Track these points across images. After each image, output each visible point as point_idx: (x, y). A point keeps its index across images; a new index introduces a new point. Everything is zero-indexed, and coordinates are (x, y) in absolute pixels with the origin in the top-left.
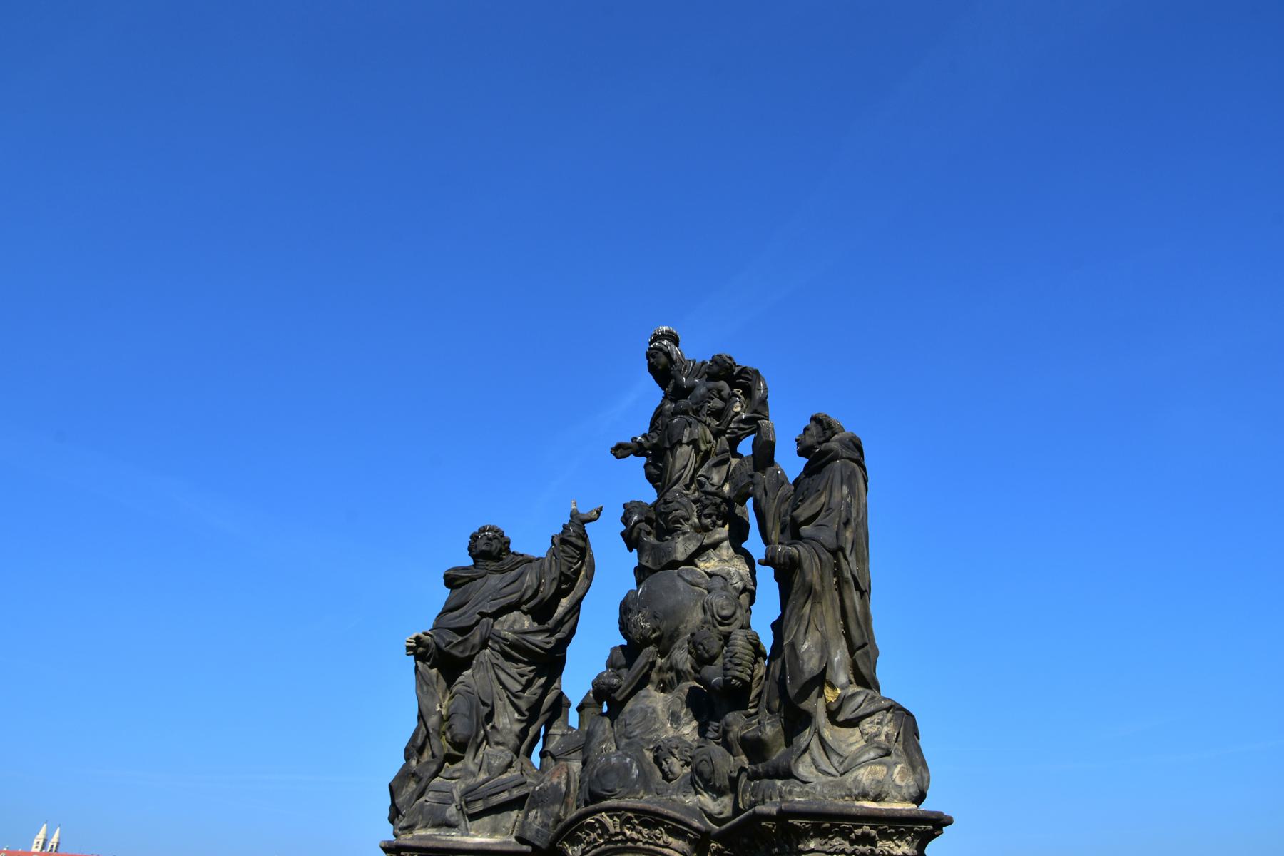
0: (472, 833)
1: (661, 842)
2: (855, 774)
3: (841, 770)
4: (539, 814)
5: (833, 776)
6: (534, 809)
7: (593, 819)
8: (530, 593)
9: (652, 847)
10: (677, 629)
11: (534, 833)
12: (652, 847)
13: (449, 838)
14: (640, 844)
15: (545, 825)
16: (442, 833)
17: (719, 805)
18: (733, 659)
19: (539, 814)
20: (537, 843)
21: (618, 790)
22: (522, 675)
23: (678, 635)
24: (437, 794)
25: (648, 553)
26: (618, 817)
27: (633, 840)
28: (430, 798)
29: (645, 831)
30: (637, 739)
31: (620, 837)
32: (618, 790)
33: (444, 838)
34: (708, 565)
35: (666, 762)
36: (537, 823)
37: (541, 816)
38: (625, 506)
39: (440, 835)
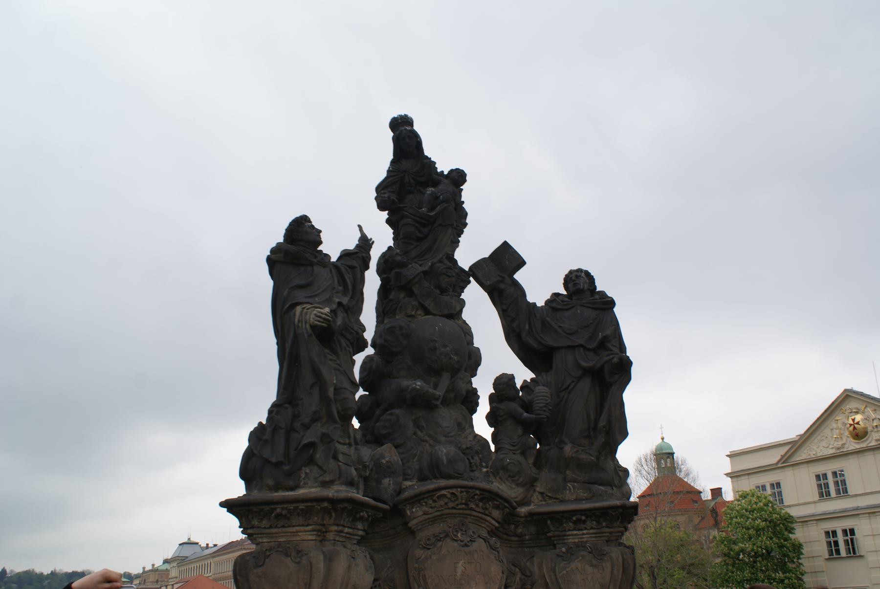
1: (487, 512)
6: (386, 477)
7: (447, 492)
9: (480, 515)
12: (480, 515)
14: (475, 513)
19: (391, 482)
26: (467, 492)
27: (472, 509)
29: (481, 504)
37: (393, 483)
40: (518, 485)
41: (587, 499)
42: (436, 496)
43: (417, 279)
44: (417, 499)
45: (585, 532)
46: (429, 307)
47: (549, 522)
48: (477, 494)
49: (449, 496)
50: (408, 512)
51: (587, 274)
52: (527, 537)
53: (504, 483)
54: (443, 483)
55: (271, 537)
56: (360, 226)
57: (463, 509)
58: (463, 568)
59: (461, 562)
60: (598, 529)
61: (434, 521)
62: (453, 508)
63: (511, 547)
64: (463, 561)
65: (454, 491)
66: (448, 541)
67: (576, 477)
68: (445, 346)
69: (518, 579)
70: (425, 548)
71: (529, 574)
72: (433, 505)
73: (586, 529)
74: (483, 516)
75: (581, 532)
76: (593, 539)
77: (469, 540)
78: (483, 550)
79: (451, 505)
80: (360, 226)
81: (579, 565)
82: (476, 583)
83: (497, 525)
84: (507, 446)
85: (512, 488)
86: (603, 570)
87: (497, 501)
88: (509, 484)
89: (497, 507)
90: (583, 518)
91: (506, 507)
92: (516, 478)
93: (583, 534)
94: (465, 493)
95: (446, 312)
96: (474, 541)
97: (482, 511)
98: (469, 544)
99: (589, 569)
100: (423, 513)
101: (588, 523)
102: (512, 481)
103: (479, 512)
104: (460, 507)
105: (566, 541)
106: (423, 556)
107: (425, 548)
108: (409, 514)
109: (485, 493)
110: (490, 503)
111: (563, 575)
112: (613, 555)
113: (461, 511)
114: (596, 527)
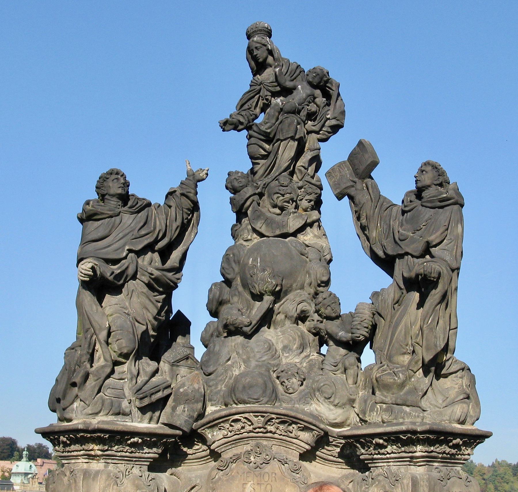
1: (292, 435)
5: (438, 408)
6: (180, 404)
8: (161, 235)
9: (284, 438)
10: (291, 286)
12: (284, 438)
14: (276, 436)
17: (334, 414)
18: (362, 323)
19: (186, 409)
20: (185, 429)
21: (261, 399)
23: (291, 291)
24: (113, 390)
25: (263, 221)
27: (271, 432)
28: (109, 393)
29: (281, 427)
31: (262, 430)
32: (261, 399)
33: (122, 423)
34: (305, 238)
36: (185, 415)
39: (118, 421)
42: (231, 420)
43: (248, 203)
44: (214, 424)
45: (388, 456)
48: (273, 418)
49: (244, 420)
50: (210, 436)
51: (435, 167)
53: (322, 404)
54: (241, 407)
58: (252, 489)
59: (250, 483)
62: (251, 432)
64: (252, 482)
65: (246, 415)
67: (384, 398)
72: (231, 428)
73: (388, 453)
77: (261, 462)
78: (276, 472)
79: (248, 428)
88: (327, 405)
89: (305, 429)
90: (381, 441)
92: (331, 400)
93: (388, 458)
94: (260, 417)
95: (278, 232)
97: (286, 434)
98: (261, 466)
104: (257, 430)
109: (282, 417)
113: (261, 434)
114: (396, 452)
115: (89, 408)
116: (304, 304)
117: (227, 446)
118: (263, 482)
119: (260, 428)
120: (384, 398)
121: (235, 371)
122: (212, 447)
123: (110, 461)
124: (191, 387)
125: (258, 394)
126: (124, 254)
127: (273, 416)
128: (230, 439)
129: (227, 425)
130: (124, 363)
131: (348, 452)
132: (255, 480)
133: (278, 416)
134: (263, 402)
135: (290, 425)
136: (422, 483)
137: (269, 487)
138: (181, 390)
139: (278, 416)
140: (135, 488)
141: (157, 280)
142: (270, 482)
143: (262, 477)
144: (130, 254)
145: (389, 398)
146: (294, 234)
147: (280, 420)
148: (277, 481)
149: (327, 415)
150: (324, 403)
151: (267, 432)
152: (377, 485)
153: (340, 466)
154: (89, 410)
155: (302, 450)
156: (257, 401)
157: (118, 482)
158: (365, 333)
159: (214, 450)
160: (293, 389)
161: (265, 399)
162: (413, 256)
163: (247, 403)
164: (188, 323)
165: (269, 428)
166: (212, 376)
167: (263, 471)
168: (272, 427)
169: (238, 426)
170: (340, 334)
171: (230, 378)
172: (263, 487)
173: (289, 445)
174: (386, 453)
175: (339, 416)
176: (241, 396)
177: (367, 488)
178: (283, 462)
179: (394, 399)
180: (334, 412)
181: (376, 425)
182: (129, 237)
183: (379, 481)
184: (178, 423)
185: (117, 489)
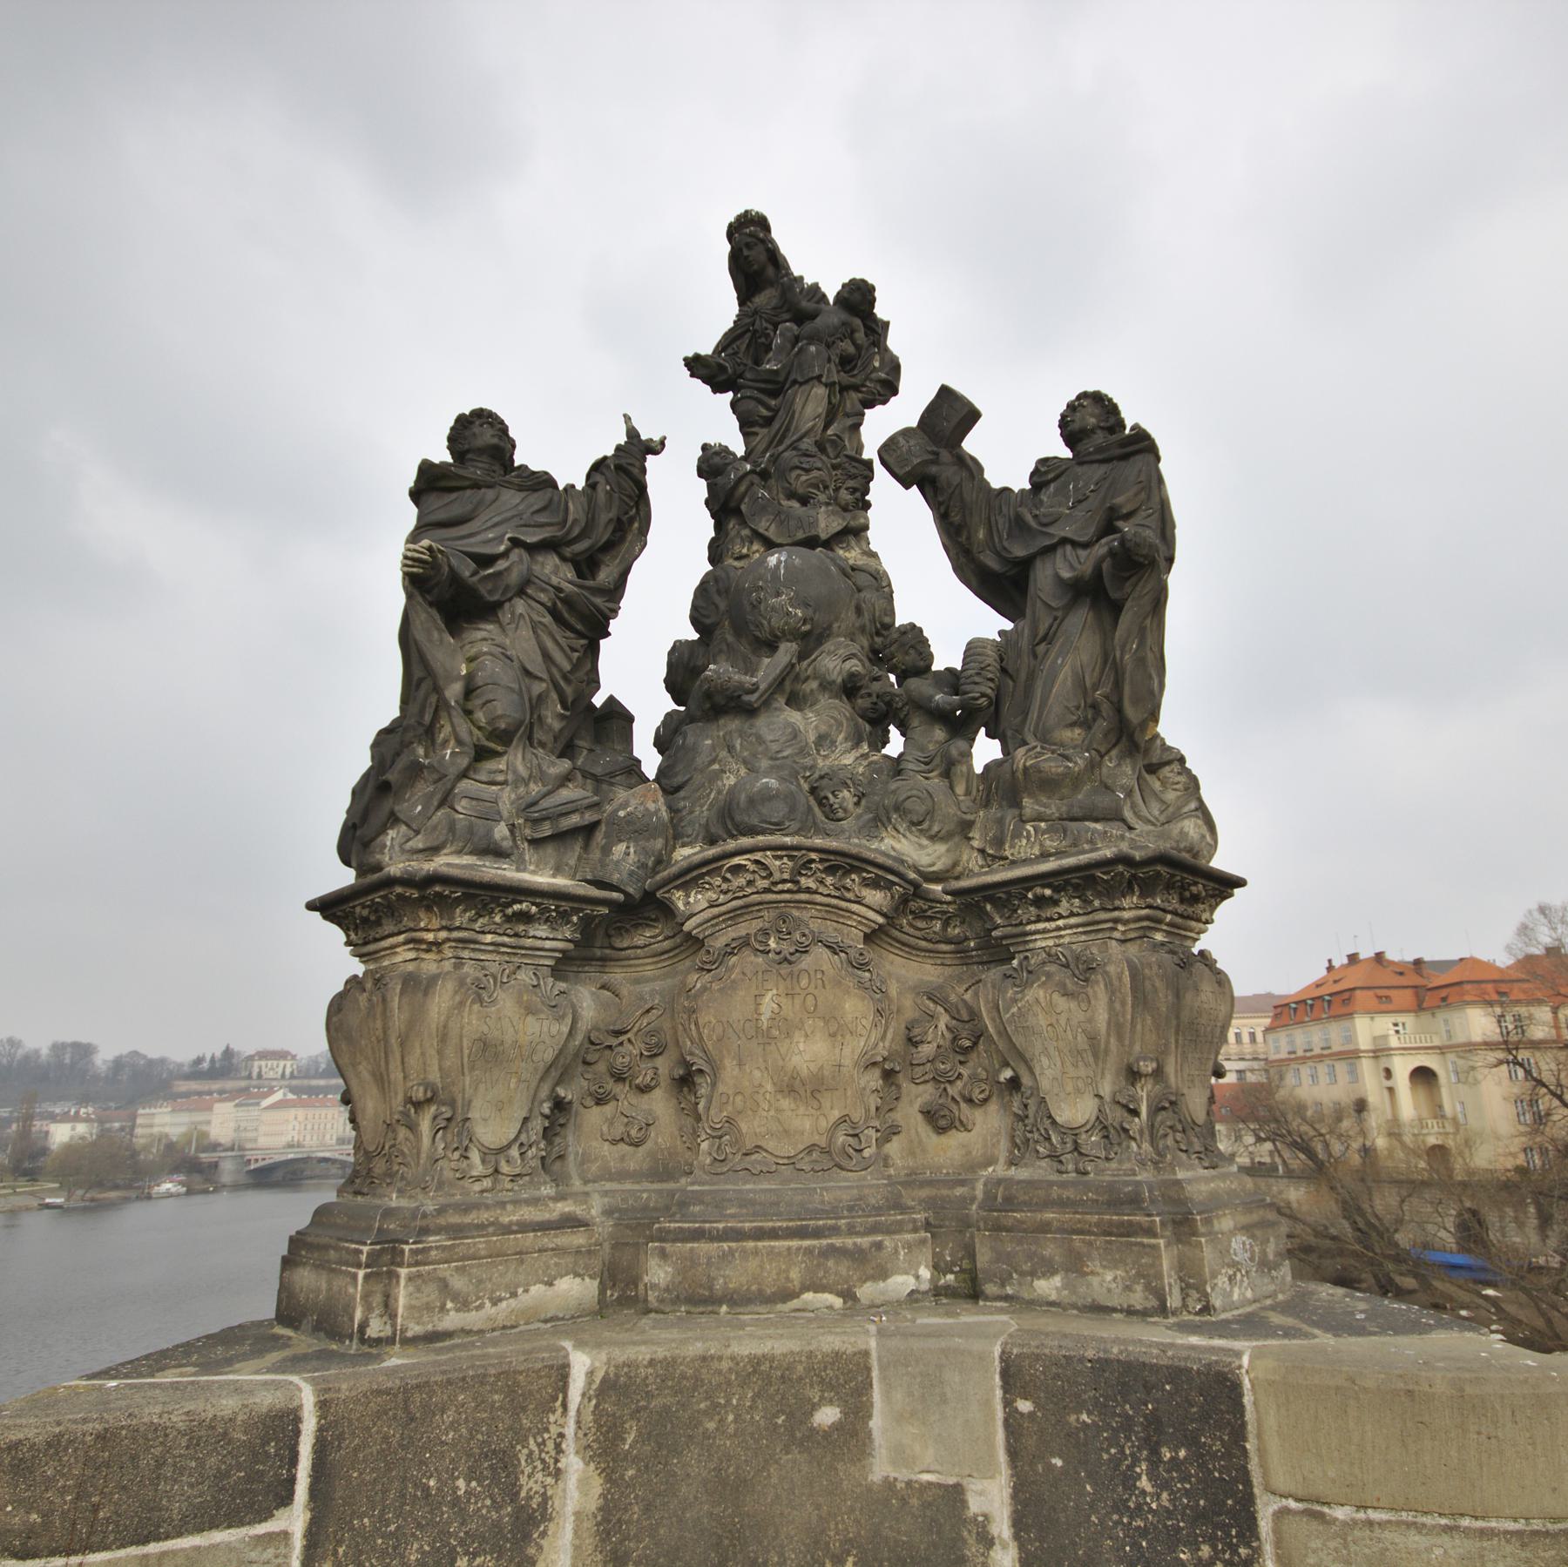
0: (532, 868)
1: (849, 895)
2: (1180, 825)
3: (1162, 819)
4: (632, 850)
5: (1153, 824)
6: (621, 841)
8: (576, 531)
10: (830, 627)
11: (625, 876)
13: (499, 872)
14: (819, 898)
15: (643, 866)
16: (487, 864)
19: (632, 850)
20: (631, 890)
21: (787, 824)
22: (574, 650)
24: (474, 803)
26: (791, 858)
27: (808, 890)
28: (464, 808)
29: (829, 880)
30: (788, 762)
31: (789, 885)
32: (787, 824)
35: (835, 796)
38: (705, 447)
39: (484, 866)
40: (933, 838)
41: (1059, 854)
44: (690, 877)
45: (1060, 923)
46: (766, 533)
47: (989, 907)
48: (813, 861)
49: (752, 867)
50: (680, 905)
52: (972, 944)
53: (904, 836)
54: (745, 841)
55: (376, 960)
56: (627, 418)
57: (788, 891)
59: (770, 994)
60: (1085, 914)
61: (735, 915)
62: (767, 891)
63: (942, 964)
65: (758, 856)
66: (746, 952)
67: (1043, 809)
68: (778, 594)
69: (942, 1026)
70: (703, 969)
71: (966, 1017)
72: (725, 886)
73: (1061, 917)
74: (844, 904)
75: (1053, 925)
76: (1083, 938)
77: (792, 950)
78: (824, 968)
79: (762, 884)
80: (627, 418)
81: (1041, 993)
82: (807, 1036)
83: (881, 920)
84: (911, 766)
85: (922, 847)
86: (1089, 1002)
87: (869, 872)
88: (914, 839)
89: (875, 884)
90: (1048, 892)
91: (895, 884)
92: (925, 826)
93: (1059, 929)
94: (785, 860)
96: (806, 952)
98: (792, 958)
99: (1061, 1003)
100: (706, 905)
101: (1064, 903)
102: (921, 831)
103: (829, 895)
104: (780, 887)
105: (1031, 946)
106: (698, 985)
107: (703, 969)
108: (682, 908)
109: (832, 857)
110: (853, 876)
111: (1013, 1015)
112: (1111, 969)
113: (787, 896)
115: (419, 837)
116: (854, 661)
117: (717, 924)
118: (798, 990)
119: (784, 881)
120: (1043, 809)
121: (728, 778)
122: (687, 927)
123: (466, 954)
124: (642, 808)
125: (781, 814)
126: (502, 548)
127: (813, 856)
128: (723, 909)
129: (718, 881)
130: (499, 754)
131: (957, 931)
132: (782, 987)
133: (824, 856)
134: (791, 830)
135: (847, 873)
136: (1147, 971)
137: (810, 1000)
138: (622, 814)
139: (824, 856)
140: (522, 1011)
141: (568, 601)
142: (811, 990)
143: (795, 980)
144: (517, 551)
145: (1054, 810)
146: (828, 544)
147: (827, 864)
148: (828, 987)
149: (915, 857)
150: (908, 834)
151: (799, 891)
152: (1044, 983)
153: (939, 962)
154: (418, 842)
155: (870, 927)
156: (778, 827)
157: (485, 995)
158: (989, 691)
159: (689, 933)
160: (845, 810)
161: (795, 826)
162: (1075, 544)
163: (758, 834)
164: (629, 719)
165: (805, 882)
166: (682, 794)
167: (796, 968)
168: (810, 880)
169: (741, 881)
170: (937, 697)
171: (719, 792)
172: (798, 1001)
173: (843, 916)
174: (1056, 916)
175: (939, 858)
176: (746, 819)
177: (1017, 993)
178: (834, 949)
179: (1064, 809)
180: (930, 850)
181: (1026, 861)
182: (516, 521)
183: (1049, 975)
184: (615, 878)
185: (479, 1012)
